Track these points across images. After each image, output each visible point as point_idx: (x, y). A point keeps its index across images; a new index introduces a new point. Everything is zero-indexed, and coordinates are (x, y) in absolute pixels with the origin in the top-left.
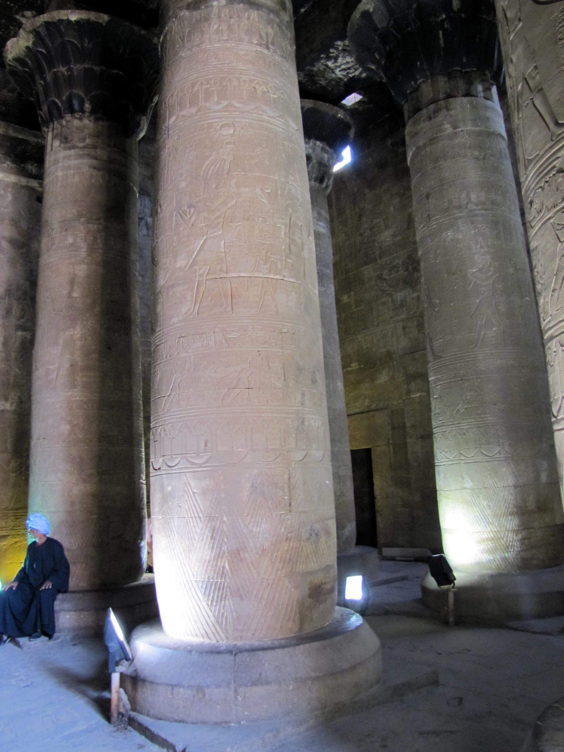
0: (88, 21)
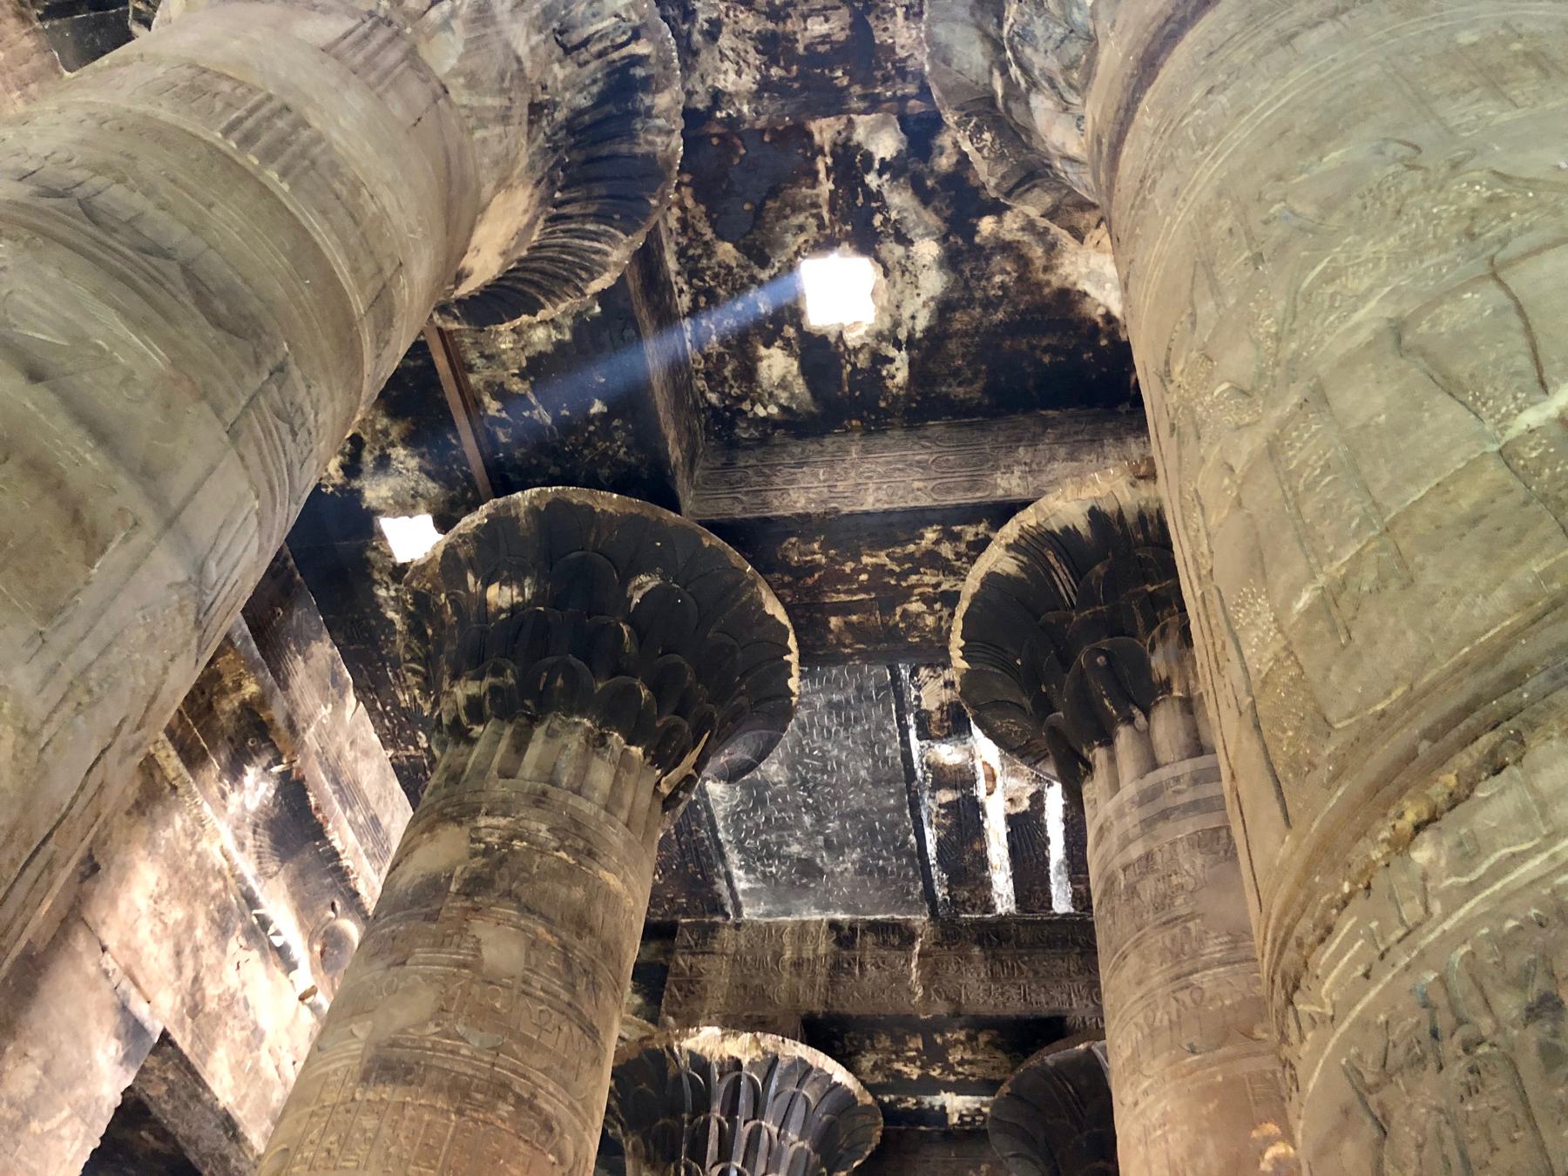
0: (849, 1091)
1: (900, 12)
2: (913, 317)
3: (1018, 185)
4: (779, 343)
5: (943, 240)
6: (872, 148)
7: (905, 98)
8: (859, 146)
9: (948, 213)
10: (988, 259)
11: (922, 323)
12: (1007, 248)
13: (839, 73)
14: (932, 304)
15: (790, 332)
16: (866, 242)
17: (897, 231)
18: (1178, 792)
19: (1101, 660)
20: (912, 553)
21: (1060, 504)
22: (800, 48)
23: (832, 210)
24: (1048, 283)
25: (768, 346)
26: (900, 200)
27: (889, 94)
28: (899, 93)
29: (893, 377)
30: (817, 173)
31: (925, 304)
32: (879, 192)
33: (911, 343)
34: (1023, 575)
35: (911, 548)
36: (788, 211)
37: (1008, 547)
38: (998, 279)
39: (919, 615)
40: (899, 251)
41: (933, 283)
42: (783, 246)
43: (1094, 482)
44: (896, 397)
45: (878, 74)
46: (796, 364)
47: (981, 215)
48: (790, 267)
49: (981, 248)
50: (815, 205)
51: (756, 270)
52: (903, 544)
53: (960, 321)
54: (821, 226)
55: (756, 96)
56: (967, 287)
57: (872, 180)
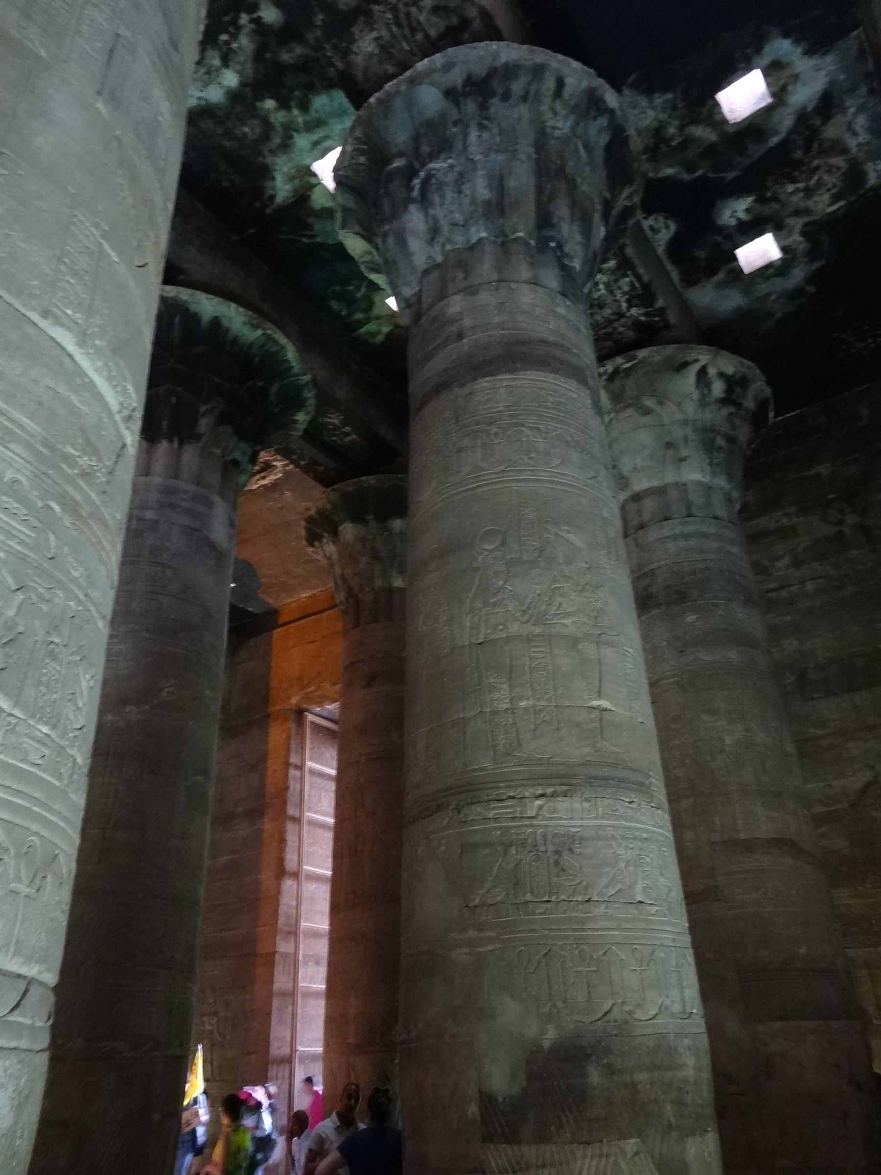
1: (375, 34)
3: (350, 187)
5: (243, 84)
7: (332, 65)
10: (253, 117)
12: (266, 124)
13: (321, 17)
14: (203, 103)
18: (183, 499)
19: (173, 400)
21: (205, 302)
24: (264, 157)
26: (245, 43)
27: (329, 54)
28: (333, 60)
31: (200, 98)
38: (246, 129)
40: (217, 62)
43: (229, 307)
45: (335, 41)
49: (255, 109)
57: (244, 19)
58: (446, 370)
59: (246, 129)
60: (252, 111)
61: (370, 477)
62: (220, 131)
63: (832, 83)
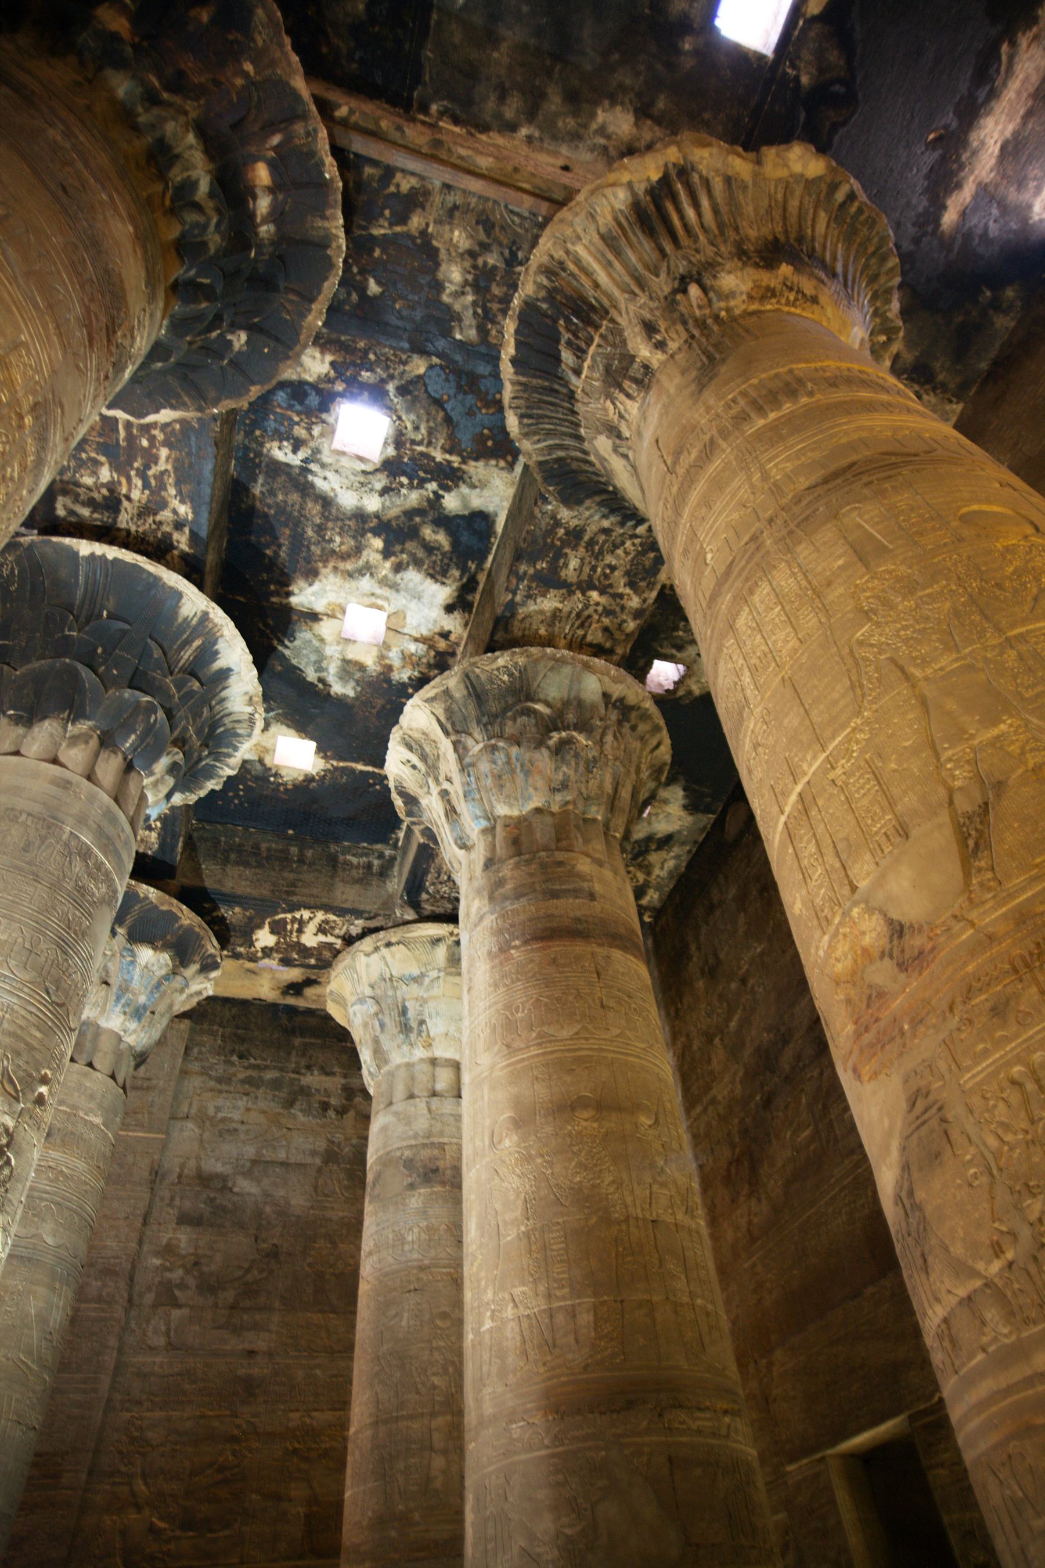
1: (560, 606)
2: (325, 478)
4: (332, 373)
5: (377, 516)
6: (453, 494)
8: (457, 486)
9: (394, 523)
10: (354, 537)
11: (319, 483)
12: (358, 550)
15: (339, 387)
16: (390, 467)
17: (393, 490)
20: (166, 489)
22: (567, 550)
23: (422, 454)
24: (325, 567)
25: (332, 364)
26: (413, 498)
29: (280, 448)
30: (451, 453)
31: (333, 490)
32: (422, 488)
33: (305, 470)
34: (180, 620)
35: (172, 491)
36: (432, 424)
37: (205, 614)
38: (338, 539)
39: (95, 474)
40: (378, 486)
41: (347, 500)
42: (408, 410)
44: (262, 445)
45: (534, 585)
46: (310, 379)
47: (385, 541)
48: (391, 409)
49: (363, 536)
50: (429, 444)
51: (396, 382)
52: (178, 484)
53: (313, 509)
54: (413, 442)
55: (554, 517)
56: (337, 519)
57: (433, 486)
58: (578, 920)
59: (338, 539)
60: (360, 533)
61: (152, 889)
62: (318, 521)
63: (679, 832)
